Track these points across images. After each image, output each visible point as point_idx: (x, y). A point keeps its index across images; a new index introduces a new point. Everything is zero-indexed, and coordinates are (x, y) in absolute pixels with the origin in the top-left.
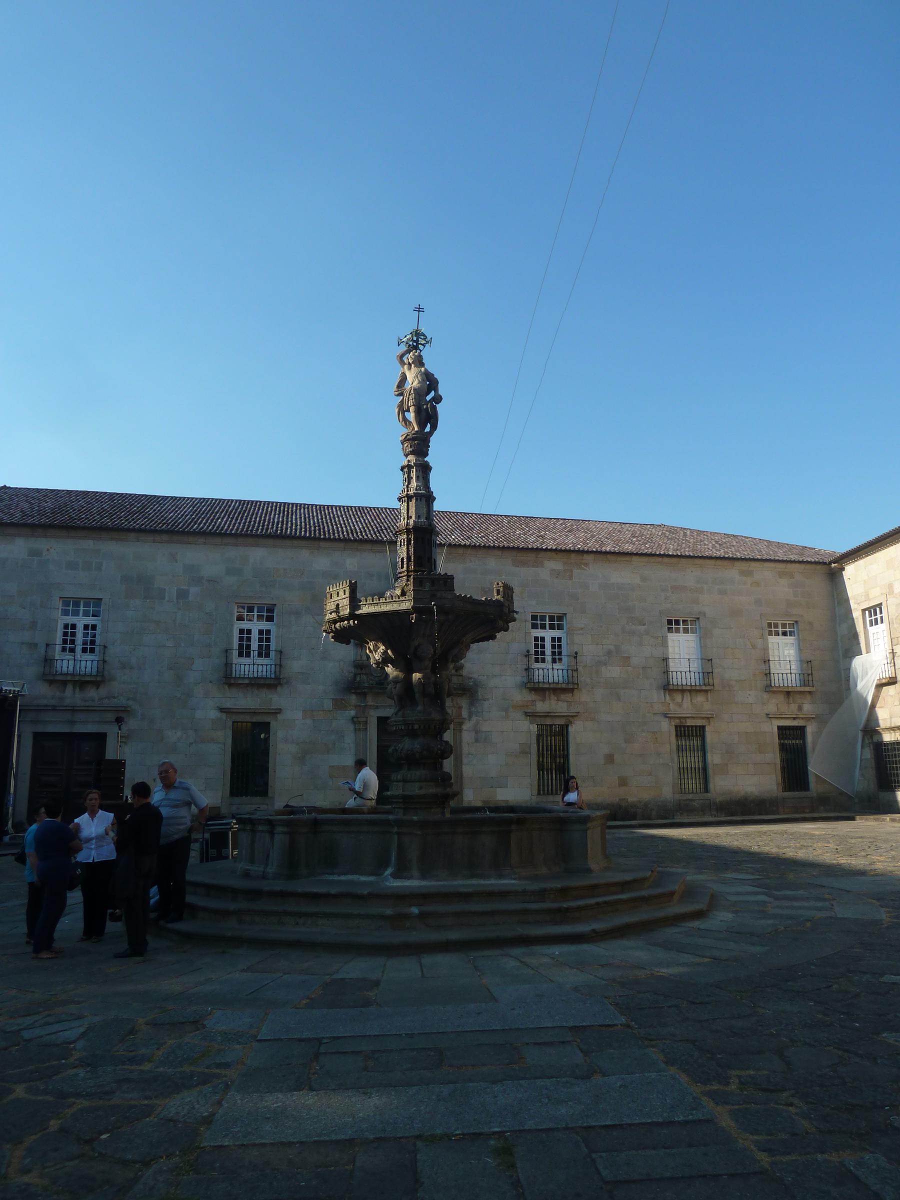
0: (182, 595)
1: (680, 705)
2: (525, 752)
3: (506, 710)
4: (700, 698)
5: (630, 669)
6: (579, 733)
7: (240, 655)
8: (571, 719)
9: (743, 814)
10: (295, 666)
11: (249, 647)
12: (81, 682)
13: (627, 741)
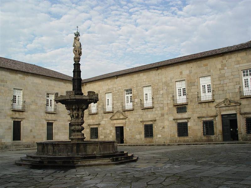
1: (48, 117)
2: (10, 129)
3: (5, 116)
4: (53, 115)
5: (37, 106)
6: (24, 124)
8: (22, 120)
9: (67, 144)
13: (35, 126)
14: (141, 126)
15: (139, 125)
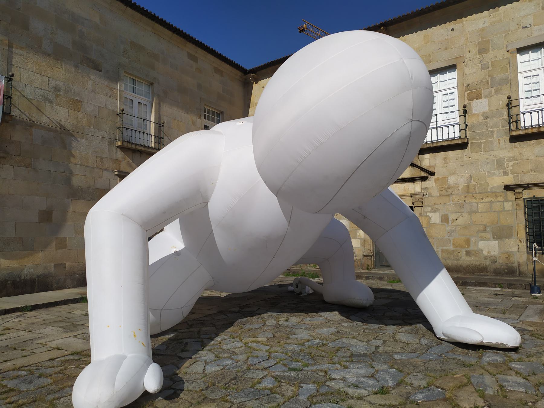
14: (508, 206)
15: (490, 199)
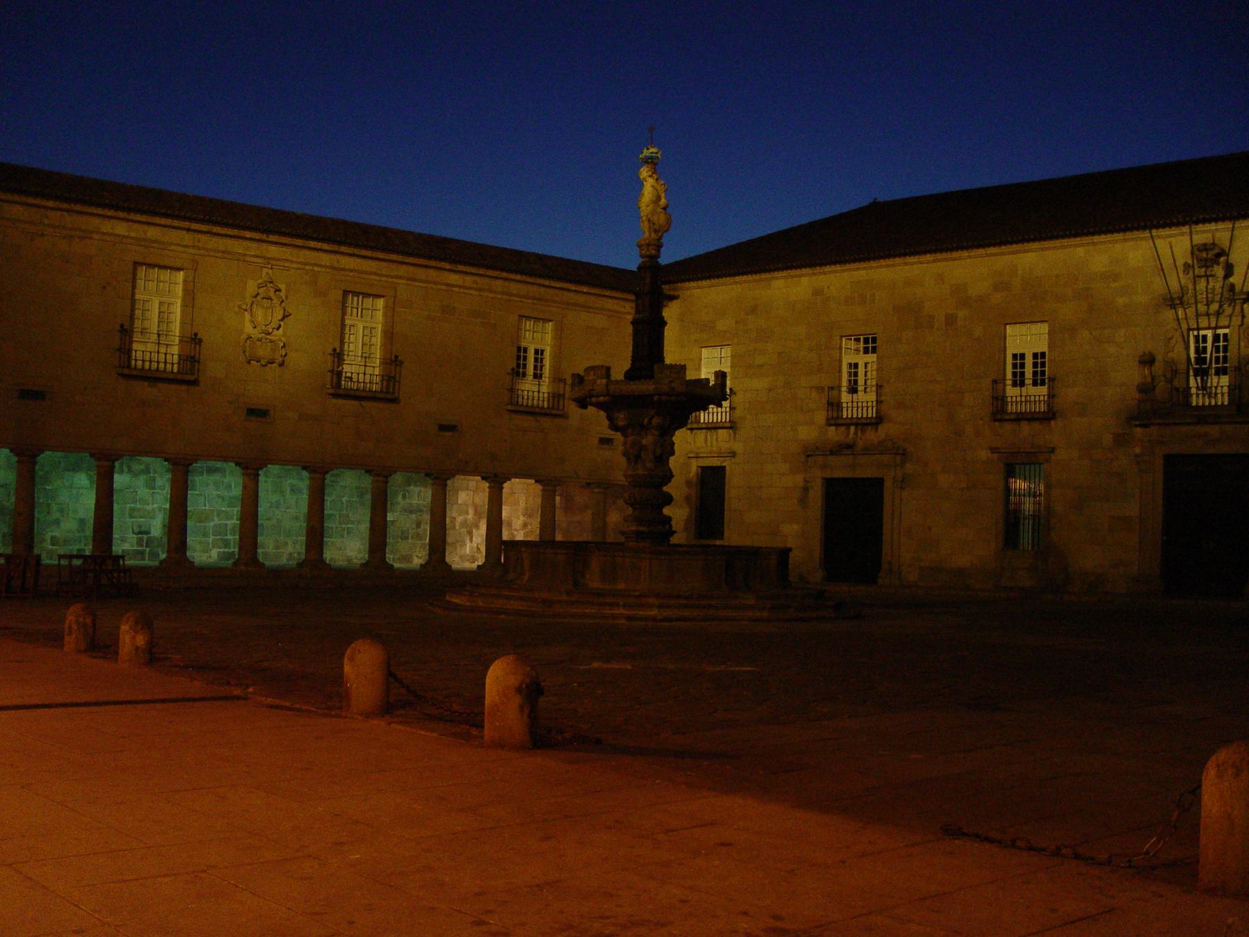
0: (951, 320)
7: (1014, 385)
10: (1070, 394)
11: (1023, 374)
12: (862, 424)
